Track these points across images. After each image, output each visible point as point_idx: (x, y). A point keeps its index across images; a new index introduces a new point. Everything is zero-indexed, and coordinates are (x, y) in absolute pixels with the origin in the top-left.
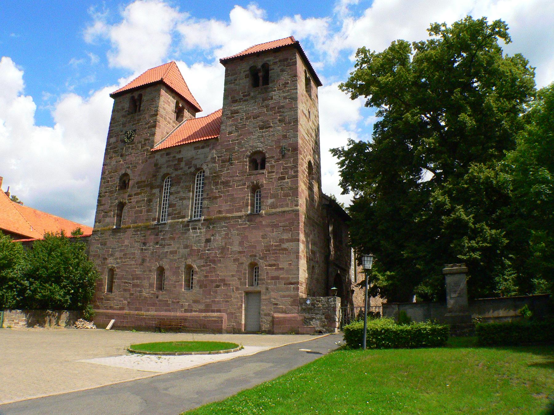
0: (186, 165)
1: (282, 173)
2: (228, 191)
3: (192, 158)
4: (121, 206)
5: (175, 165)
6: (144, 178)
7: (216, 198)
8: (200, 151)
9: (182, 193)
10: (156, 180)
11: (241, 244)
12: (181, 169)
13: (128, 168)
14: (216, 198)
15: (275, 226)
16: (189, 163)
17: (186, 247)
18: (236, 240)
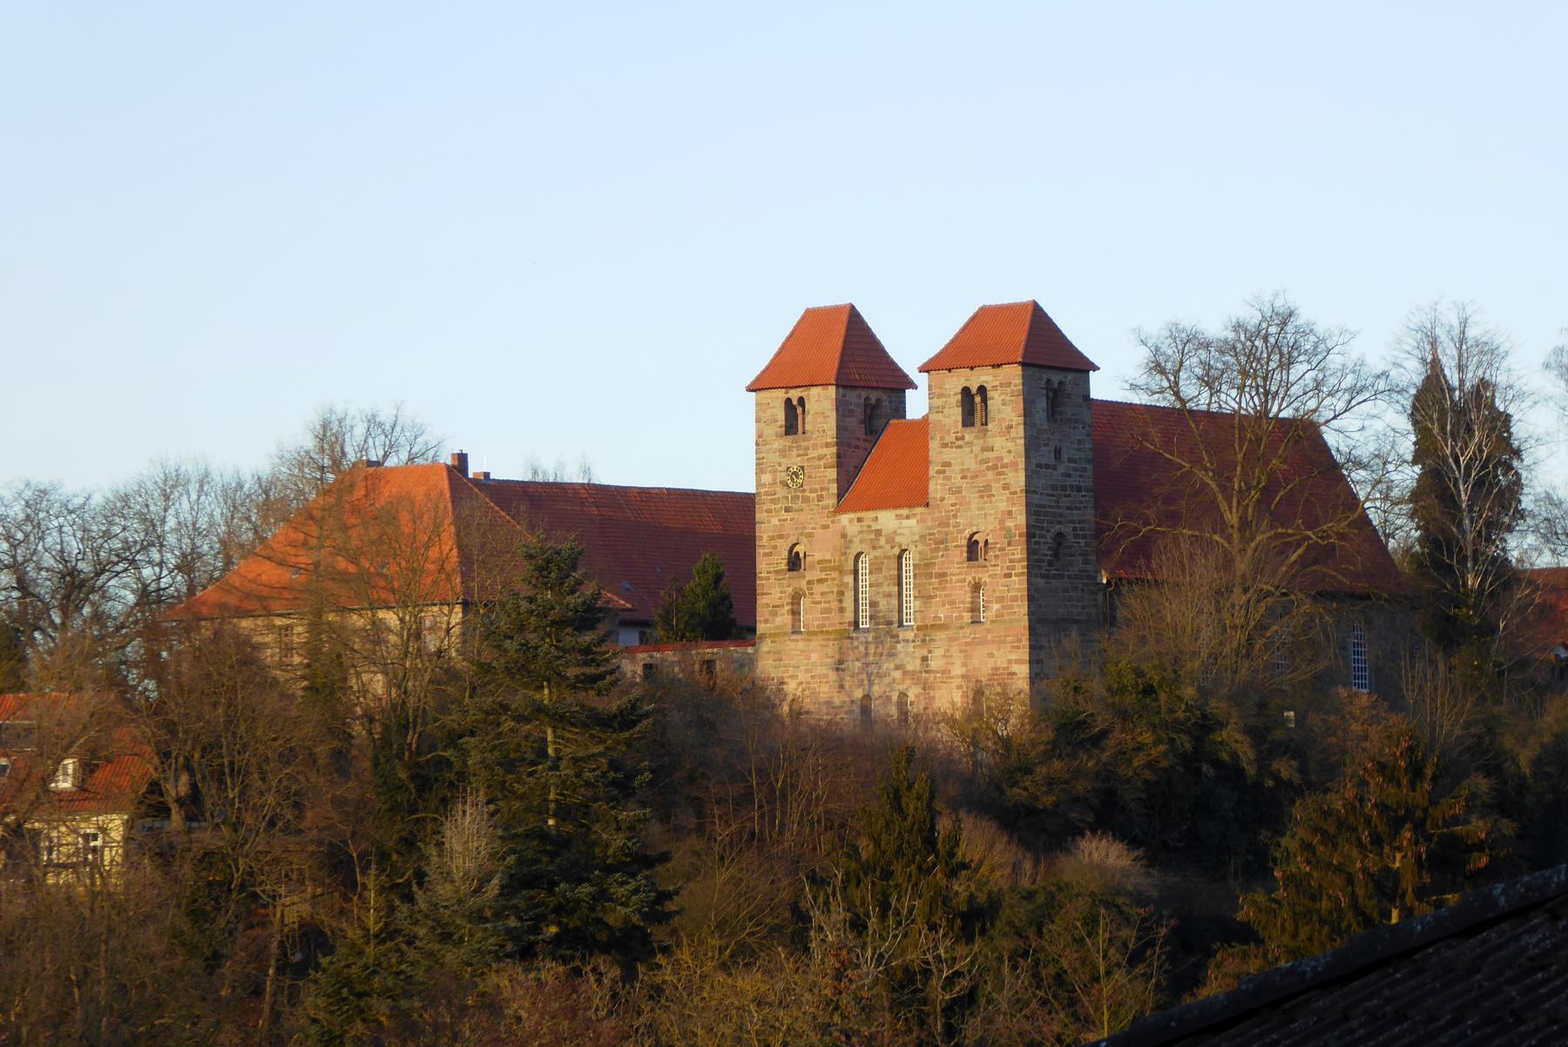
0: (887, 542)
1: (1008, 568)
2: (945, 589)
3: (895, 532)
4: (796, 598)
5: (872, 540)
6: (828, 557)
7: (930, 597)
8: (906, 523)
9: (885, 584)
10: (846, 561)
11: (964, 665)
12: (881, 547)
13: (802, 534)
14: (930, 597)
15: (1000, 642)
16: (891, 540)
17: (897, 667)
18: (958, 660)
